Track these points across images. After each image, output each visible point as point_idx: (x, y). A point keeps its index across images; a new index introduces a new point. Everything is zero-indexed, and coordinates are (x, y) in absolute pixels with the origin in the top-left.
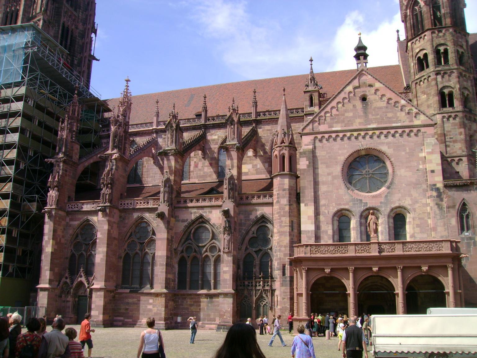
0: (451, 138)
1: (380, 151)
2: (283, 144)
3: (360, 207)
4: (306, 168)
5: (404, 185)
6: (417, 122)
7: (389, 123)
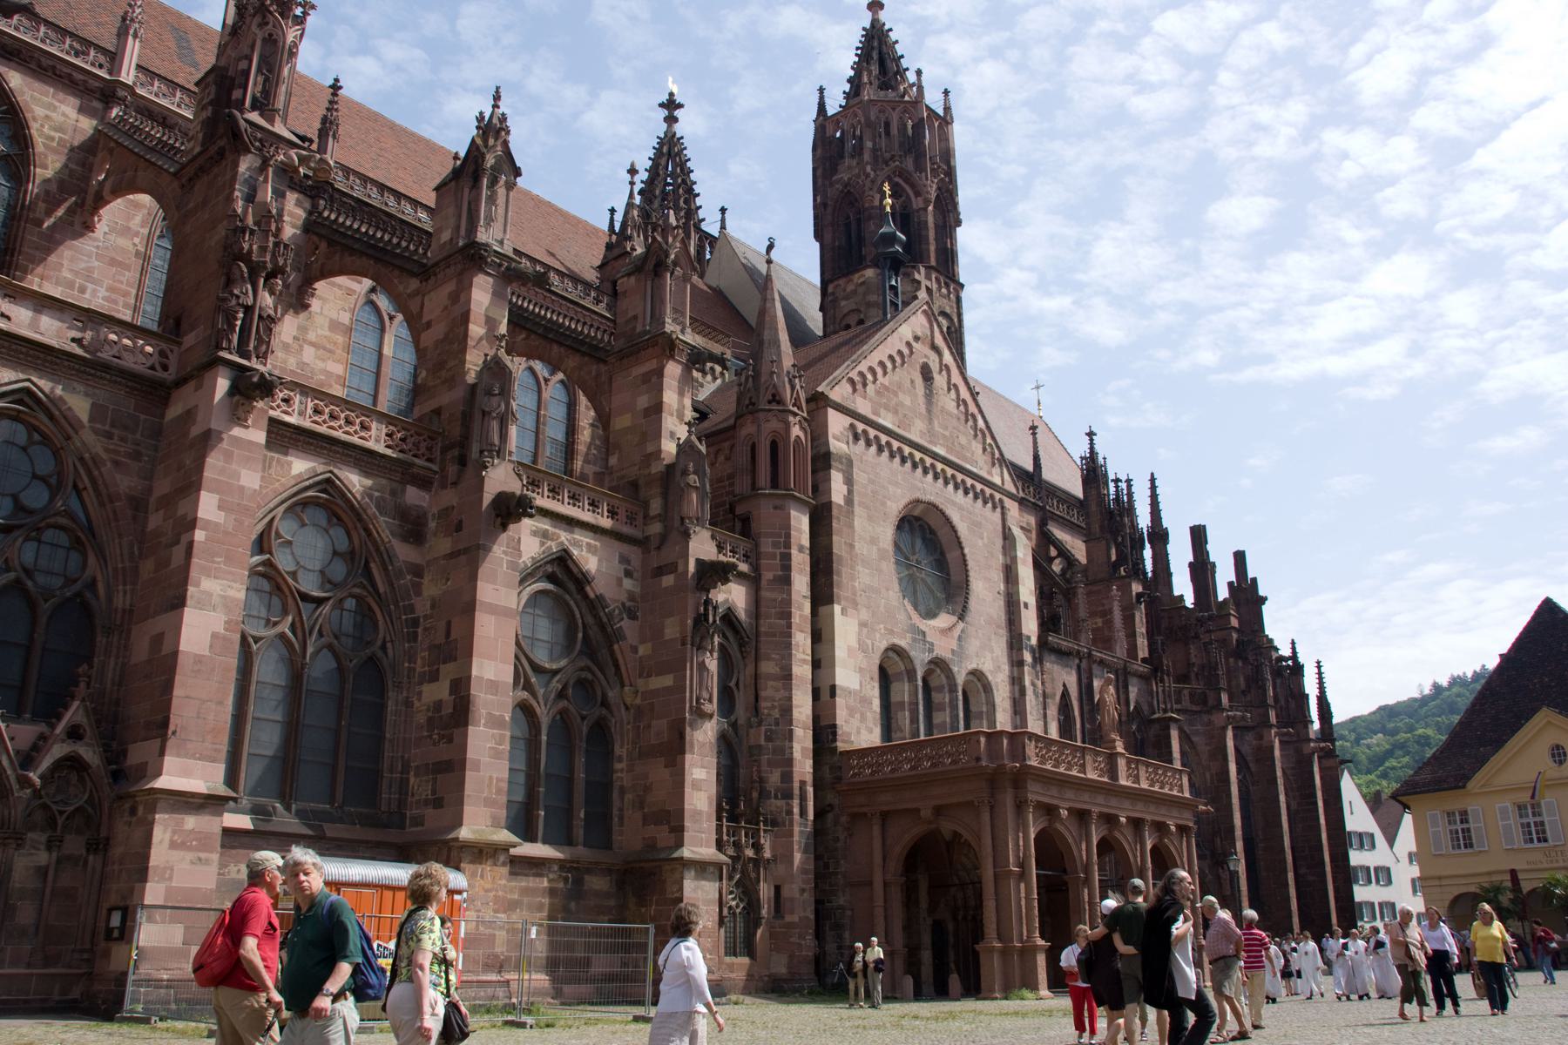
6: (997, 480)
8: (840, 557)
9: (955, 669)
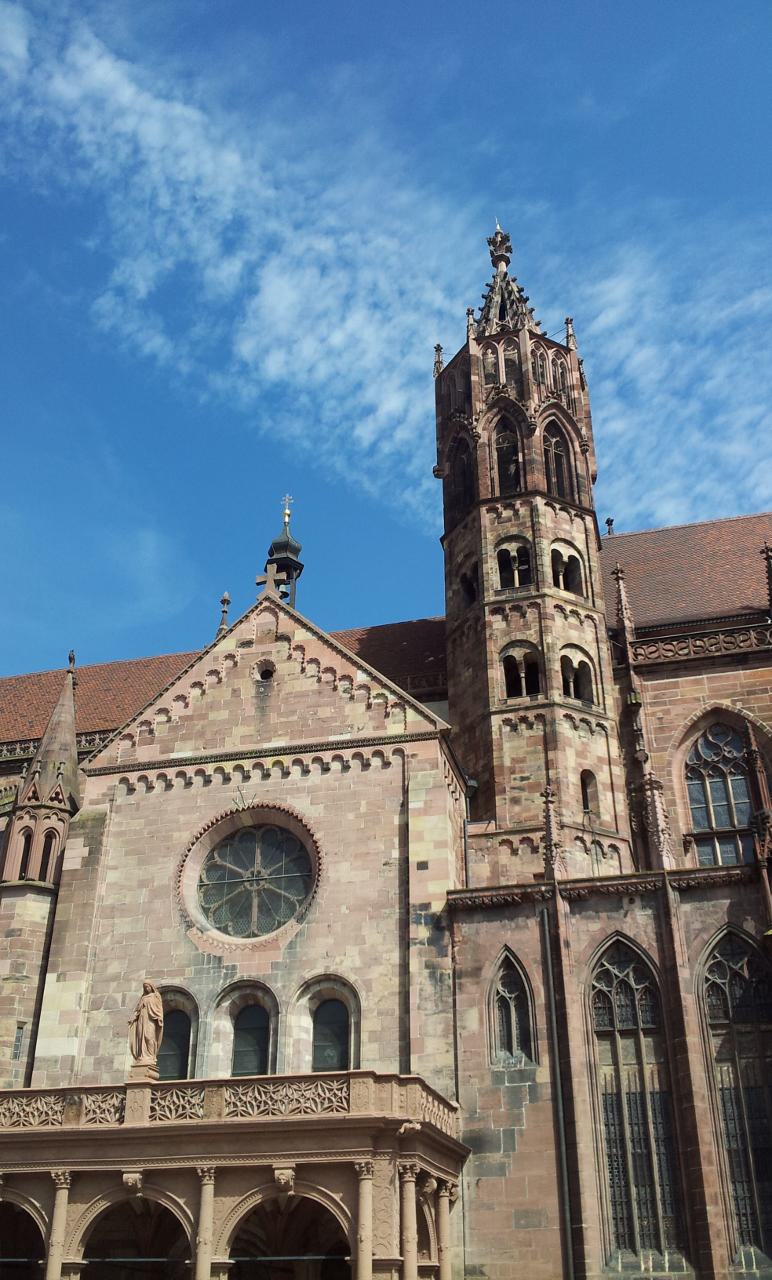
0: (523, 779)
1: (289, 814)
2: (34, 802)
3: (215, 981)
4: (79, 867)
5: (344, 909)
6: (394, 728)
7: (322, 735)
8: (65, 925)
9: (276, 986)
